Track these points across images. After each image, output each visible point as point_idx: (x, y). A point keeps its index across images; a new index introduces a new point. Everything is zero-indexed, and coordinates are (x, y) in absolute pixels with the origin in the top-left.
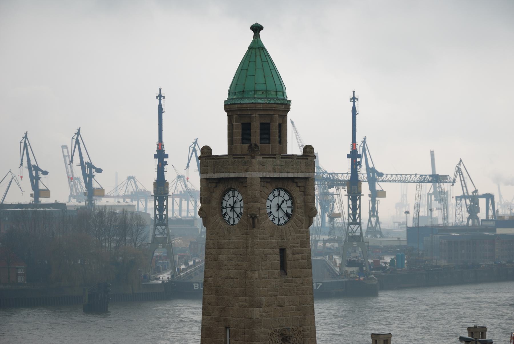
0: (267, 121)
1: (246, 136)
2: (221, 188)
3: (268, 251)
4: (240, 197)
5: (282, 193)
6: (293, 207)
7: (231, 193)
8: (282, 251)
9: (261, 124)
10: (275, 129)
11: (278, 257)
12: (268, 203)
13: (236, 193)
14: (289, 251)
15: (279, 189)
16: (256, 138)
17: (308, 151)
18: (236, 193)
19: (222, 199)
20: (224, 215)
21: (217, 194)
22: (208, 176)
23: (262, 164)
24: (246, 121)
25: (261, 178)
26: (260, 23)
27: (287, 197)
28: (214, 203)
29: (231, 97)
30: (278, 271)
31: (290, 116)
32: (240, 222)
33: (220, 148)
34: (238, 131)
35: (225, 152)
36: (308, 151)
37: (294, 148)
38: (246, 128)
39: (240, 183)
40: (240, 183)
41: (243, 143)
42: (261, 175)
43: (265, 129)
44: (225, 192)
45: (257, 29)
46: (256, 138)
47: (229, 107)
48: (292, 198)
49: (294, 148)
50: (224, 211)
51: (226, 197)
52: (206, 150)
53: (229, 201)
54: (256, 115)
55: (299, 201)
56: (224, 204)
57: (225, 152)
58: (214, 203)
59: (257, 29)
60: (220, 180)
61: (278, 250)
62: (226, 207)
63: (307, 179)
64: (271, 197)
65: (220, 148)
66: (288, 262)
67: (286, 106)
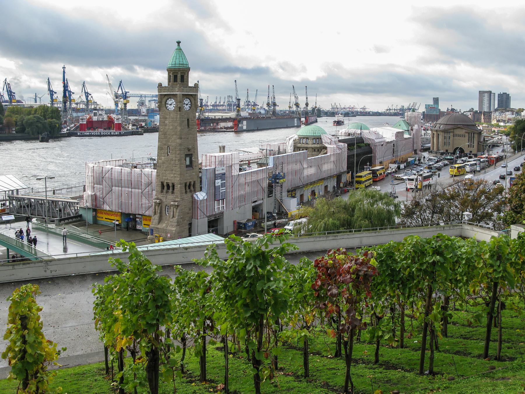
0: (183, 74)
1: (175, 80)
2: (166, 98)
3: (184, 120)
6: (191, 105)
8: (188, 120)
10: (185, 77)
14: (190, 120)
15: (187, 98)
19: (166, 101)
20: (166, 107)
21: (164, 100)
23: (183, 89)
24: (175, 74)
28: (163, 103)
32: (174, 110)
35: (167, 85)
37: (191, 84)
38: (175, 77)
39: (174, 96)
40: (174, 96)
43: (182, 77)
44: (167, 99)
45: (179, 43)
48: (191, 101)
49: (191, 84)
52: (160, 85)
53: (169, 102)
54: (179, 73)
55: (193, 102)
57: (167, 85)
58: (163, 103)
59: (179, 43)
60: (166, 95)
65: (165, 83)
66: (190, 124)
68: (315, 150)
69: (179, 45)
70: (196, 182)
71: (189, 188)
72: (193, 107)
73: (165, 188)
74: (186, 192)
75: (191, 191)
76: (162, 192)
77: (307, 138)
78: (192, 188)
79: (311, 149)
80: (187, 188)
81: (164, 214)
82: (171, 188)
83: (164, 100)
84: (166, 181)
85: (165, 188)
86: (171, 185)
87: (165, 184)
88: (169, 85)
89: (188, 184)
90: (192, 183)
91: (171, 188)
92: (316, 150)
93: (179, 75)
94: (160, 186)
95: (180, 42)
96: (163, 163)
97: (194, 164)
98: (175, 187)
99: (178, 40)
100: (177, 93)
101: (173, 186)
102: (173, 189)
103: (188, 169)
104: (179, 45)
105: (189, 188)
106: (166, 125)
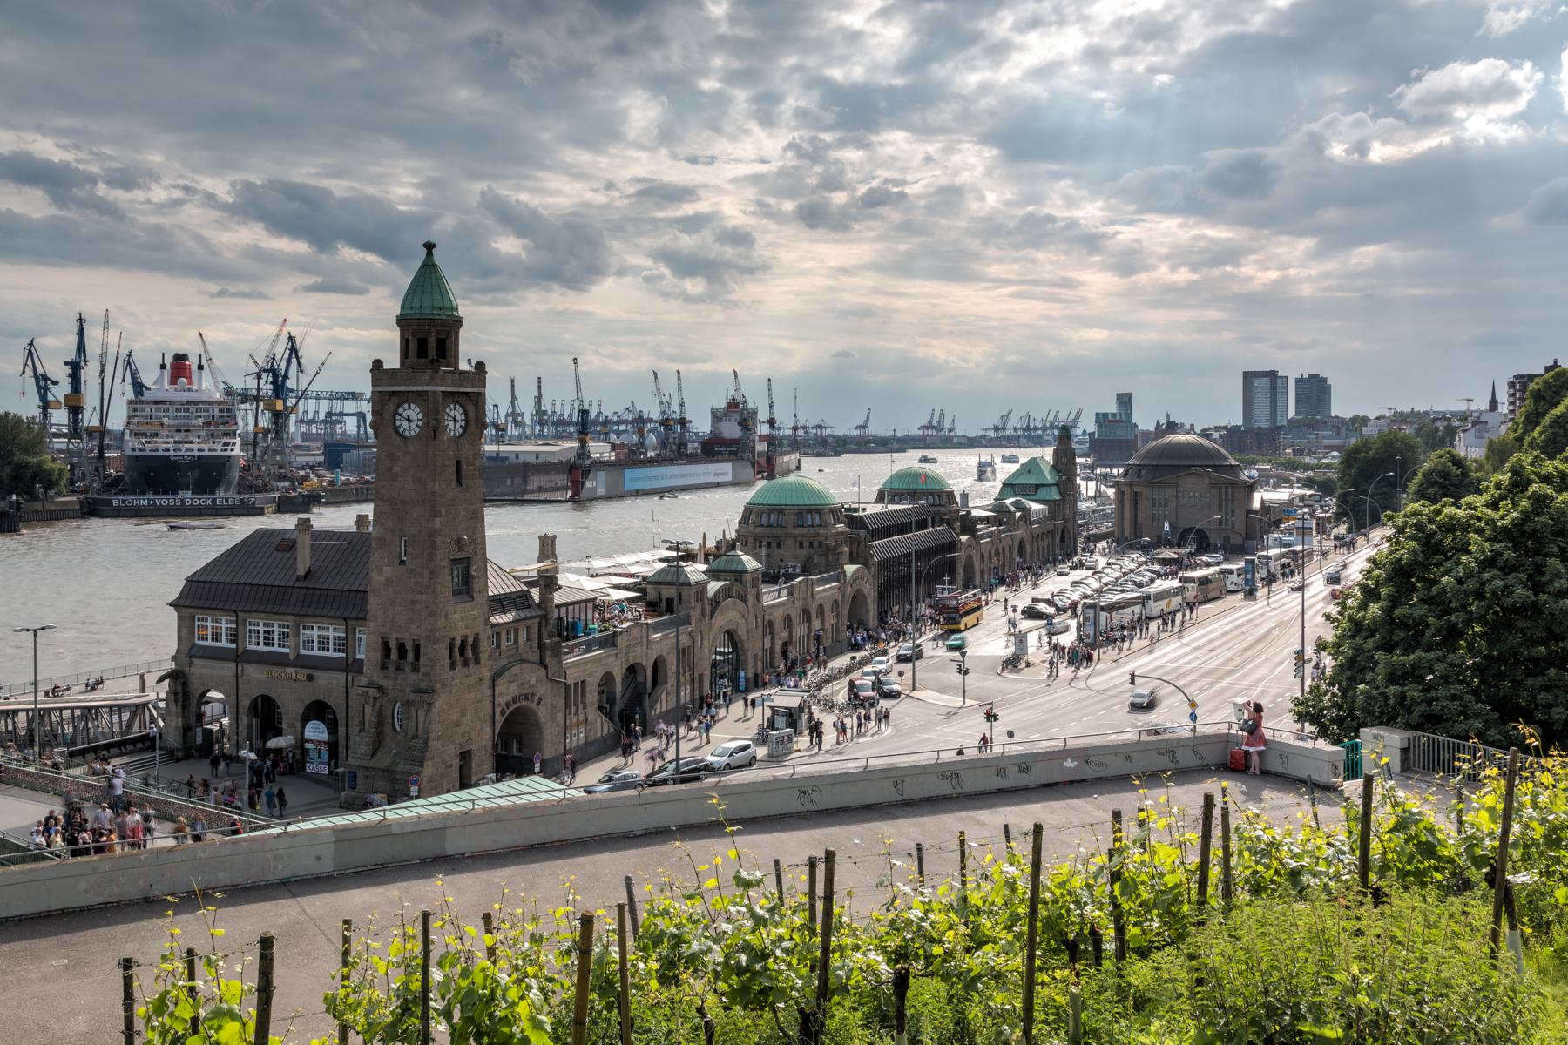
1: (422, 350)
2: (395, 400)
8: (458, 462)
11: (453, 469)
14: (464, 464)
15: (455, 403)
17: (480, 366)
30: (454, 482)
31: (462, 333)
34: (413, 346)
35: (398, 366)
39: (418, 397)
40: (418, 397)
43: (442, 344)
44: (399, 405)
47: (402, 321)
48: (465, 412)
52: (377, 364)
53: (404, 411)
55: (472, 414)
57: (398, 366)
58: (387, 415)
60: (394, 393)
65: (392, 361)
67: (457, 322)
68: (801, 545)
69: (430, 254)
70: (481, 637)
71: (462, 654)
72: (472, 428)
73: (394, 655)
74: (453, 667)
75: (466, 664)
76: (384, 667)
77: (781, 511)
78: (469, 653)
79: (790, 542)
80: (457, 654)
81: (388, 729)
82: (410, 657)
83: (391, 407)
84: (395, 635)
85: (394, 655)
86: (409, 646)
87: (393, 645)
88: (402, 364)
89: (458, 642)
90: (470, 640)
91: (410, 657)
92: (806, 544)
93: (429, 334)
94: (379, 646)
96: (388, 581)
97: (477, 586)
98: (422, 650)
100: (426, 388)
101: (417, 648)
102: (417, 657)
103: (457, 598)
104: (430, 254)
105: (462, 654)
106: (395, 477)
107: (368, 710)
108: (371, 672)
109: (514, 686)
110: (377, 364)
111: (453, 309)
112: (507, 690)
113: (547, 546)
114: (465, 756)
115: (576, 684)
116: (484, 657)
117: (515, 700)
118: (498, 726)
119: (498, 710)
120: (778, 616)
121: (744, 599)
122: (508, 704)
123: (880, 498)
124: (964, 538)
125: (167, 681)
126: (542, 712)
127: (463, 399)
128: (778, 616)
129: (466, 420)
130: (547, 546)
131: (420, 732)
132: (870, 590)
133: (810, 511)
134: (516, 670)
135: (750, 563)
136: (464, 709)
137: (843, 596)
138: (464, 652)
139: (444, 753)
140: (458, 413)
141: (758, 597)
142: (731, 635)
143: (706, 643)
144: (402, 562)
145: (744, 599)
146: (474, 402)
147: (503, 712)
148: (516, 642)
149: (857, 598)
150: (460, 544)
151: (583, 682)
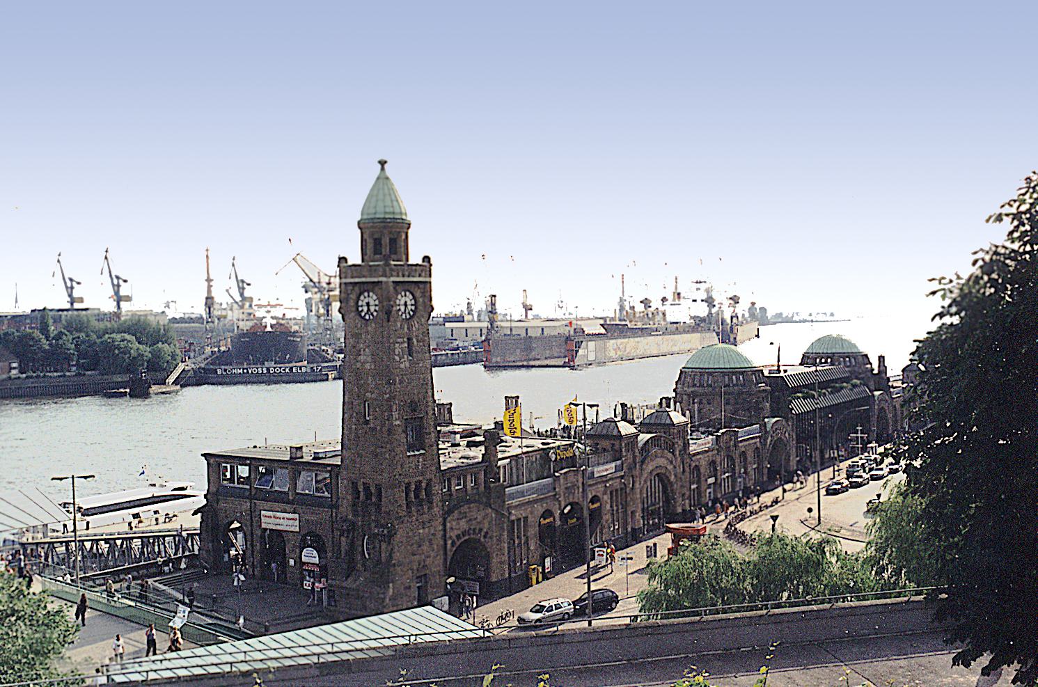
1: (377, 251)
2: (357, 289)
4: (375, 297)
5: (408, 293)
7: (366, 294)
9: (390, 239)
12: (398, 302)
13: (371, 294)
16: (386, 250)
17: (427, 259)
18: (371, 294)
19: (358, 299)
21: (353, 296)
22: (344, 281)
25: (393, 282)
26: (385, 159)
27: (411, 297)
28: (352, 303)
29: (365, 217)
33: (355, 258)
34: (370, 245)
36: (427, 259)
37: (415, 258)
38: (377, 243)
41: (375, 254)
42: (392, 279)
43: (393, 242)
45: (383, 163)
46: (386, 250)
48: (414, 297)
49: (415, 258)
50: (360, 309)
51: (362, 298)
52: (342, 260)
56: (360, 303)
59: (383, 163)
61: (405, 340)
62: (362, 306)
63: (426, 282)
64: (399, 297)
65: (355, 258)
69: (383, 169)
90: (424, 485)
95: (386, 162)
99: (379, 159)
104: (383, 169)
107: (343, 544)
108: (345, 508)
109: (463, 522)
110: (342, 260)
111: (401, 213)
112: (457, 526)
113: (512, 402)
114: (423, 577)
115: (519, 520)
116: (437, 499)
117: (464, 534)
118: (450, 554)
119: (449, 542)
120: (703, 462)
121: (671, 448)
122: (458, 537)
123: (806, 359)
124: (877, 393)
125: (199, 515)
126: (491, 544)
127: (412, 287)
128: (703, 462)
129: (415, 305)
130: (512, 402)
131: (383, 560)
132: (789, 435)
133: (734, 373)
134: (465, 508)
135: (677, 418)
136: (420, 541)
137: (764, 444)
138: (419, 496)
139: (404, 578)
140: (409, 299)
141: (686, 445)
142: (662, 478)
143: (637, 485)
144: (367, 422)
145: (671, 448)
146: (422, 291)
147: (453, 543)
148: (465, 486)
149: (778, 445)
150: (413, 406)
151: (526, 518)
